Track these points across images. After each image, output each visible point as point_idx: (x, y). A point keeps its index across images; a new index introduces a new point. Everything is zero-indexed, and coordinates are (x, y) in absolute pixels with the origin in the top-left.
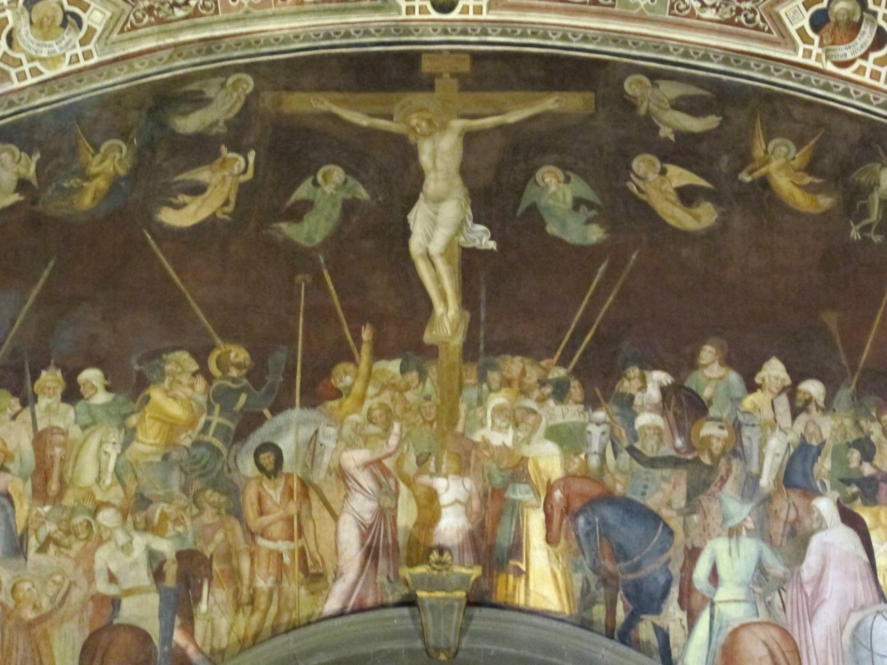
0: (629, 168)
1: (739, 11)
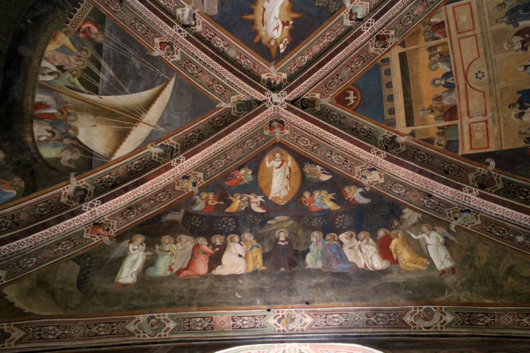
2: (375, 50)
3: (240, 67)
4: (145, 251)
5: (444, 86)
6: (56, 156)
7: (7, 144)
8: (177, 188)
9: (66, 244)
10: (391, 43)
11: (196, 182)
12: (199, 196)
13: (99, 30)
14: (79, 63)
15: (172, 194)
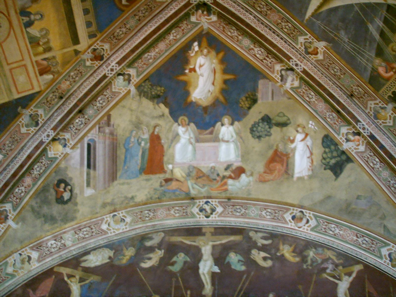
0: (251, 253)
1: (275, 216)
2: (103, 46)
3: (238, 28)
5: (30, 13)
10: (88, 53)
13: (377, 69)
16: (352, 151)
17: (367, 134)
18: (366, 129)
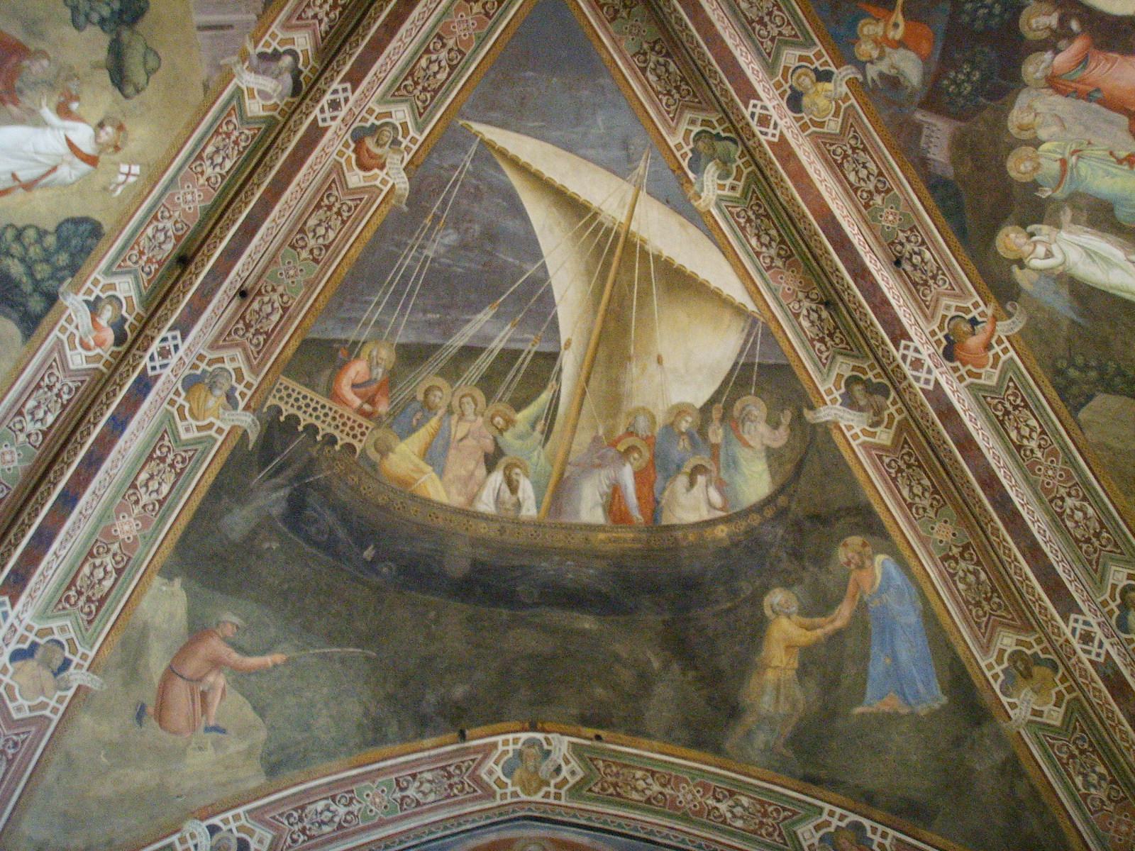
4: (1058, 226)
6: (764, 460)
7: (743, 584)
8: (833, 126)
9: (1018, 429)
11: (816, 70)
12: (868, 65)
13: (358, 356)
14: (469, 408)
15: (853, 142)
16: (63, 330)
17: (149, 365)
18: (165, 361)
